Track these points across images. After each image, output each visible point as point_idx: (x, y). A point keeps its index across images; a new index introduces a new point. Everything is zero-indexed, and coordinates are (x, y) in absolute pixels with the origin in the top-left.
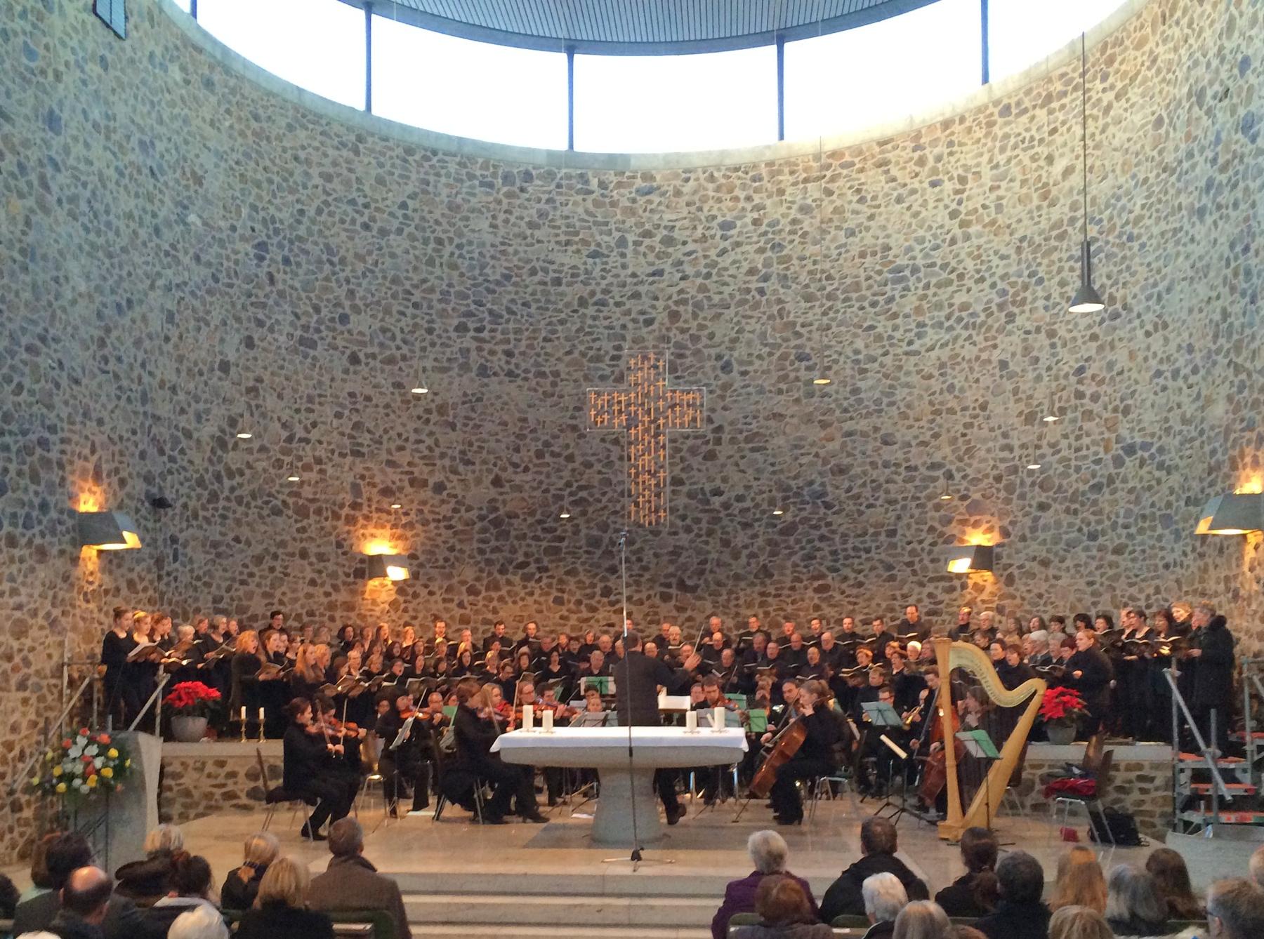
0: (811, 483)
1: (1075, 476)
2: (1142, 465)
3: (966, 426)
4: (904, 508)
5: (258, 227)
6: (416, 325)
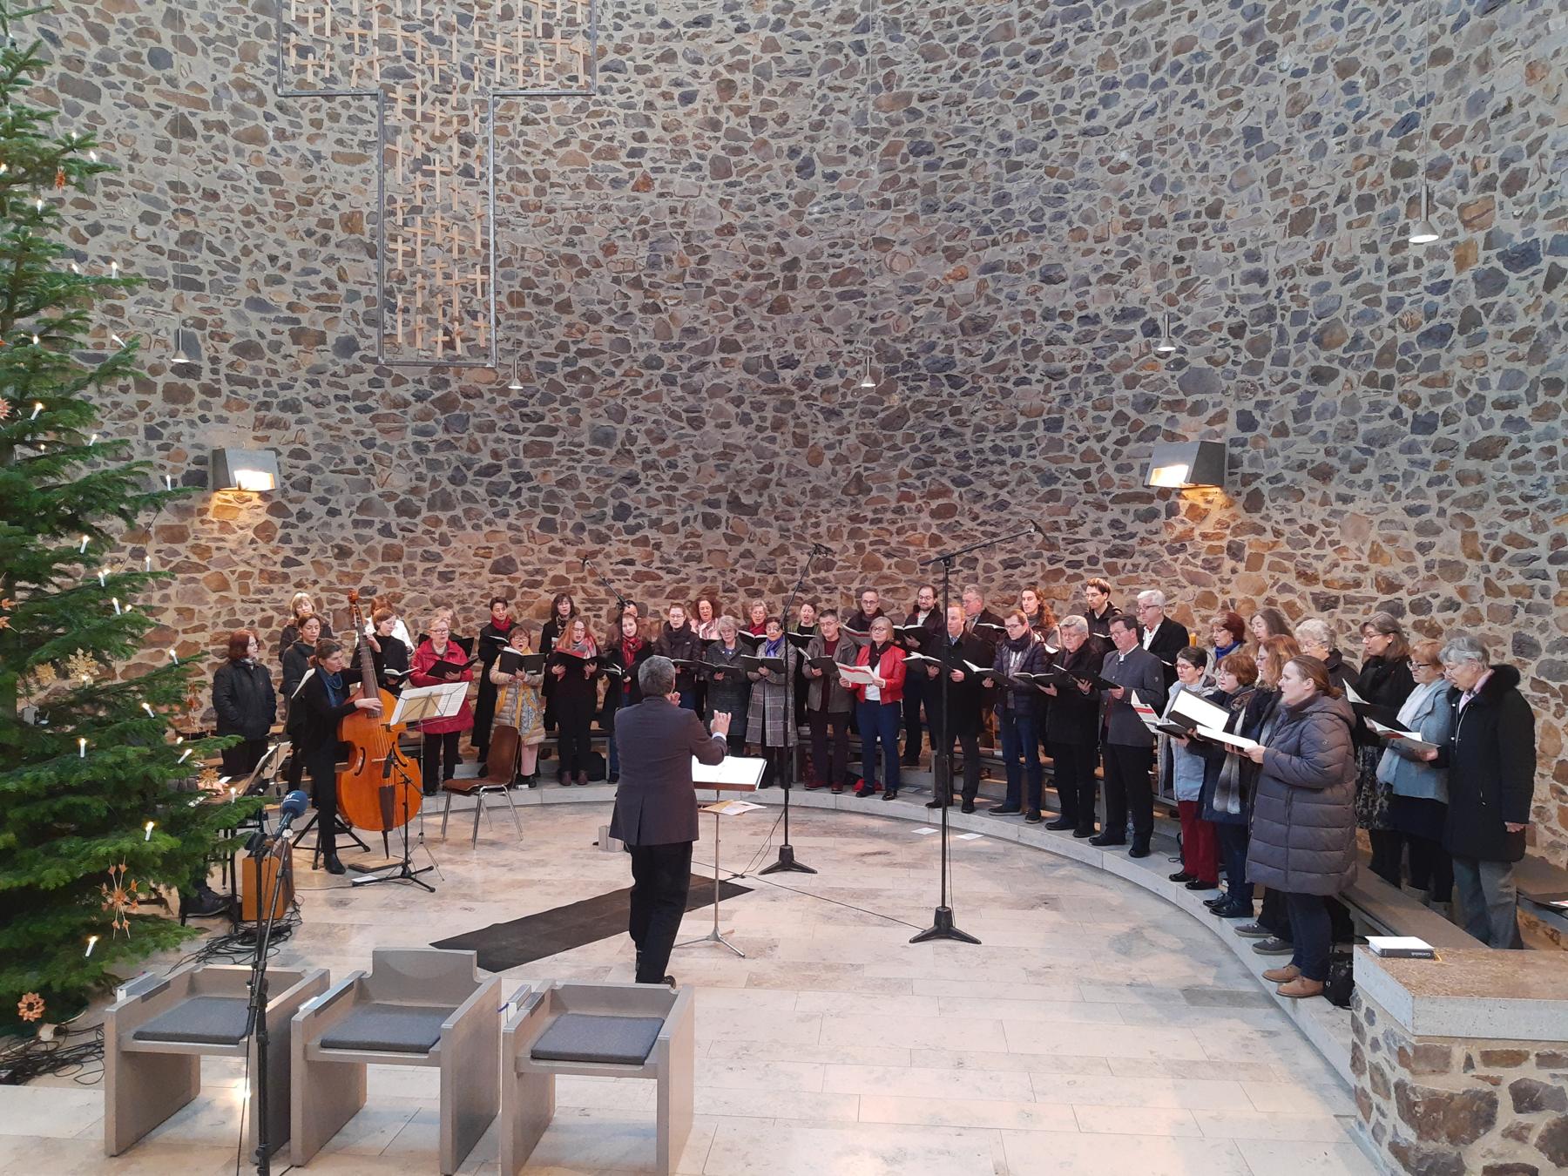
0: (932, 346)
1: (1388, 318)
3: (1182, 245)
4: (1076, 383)
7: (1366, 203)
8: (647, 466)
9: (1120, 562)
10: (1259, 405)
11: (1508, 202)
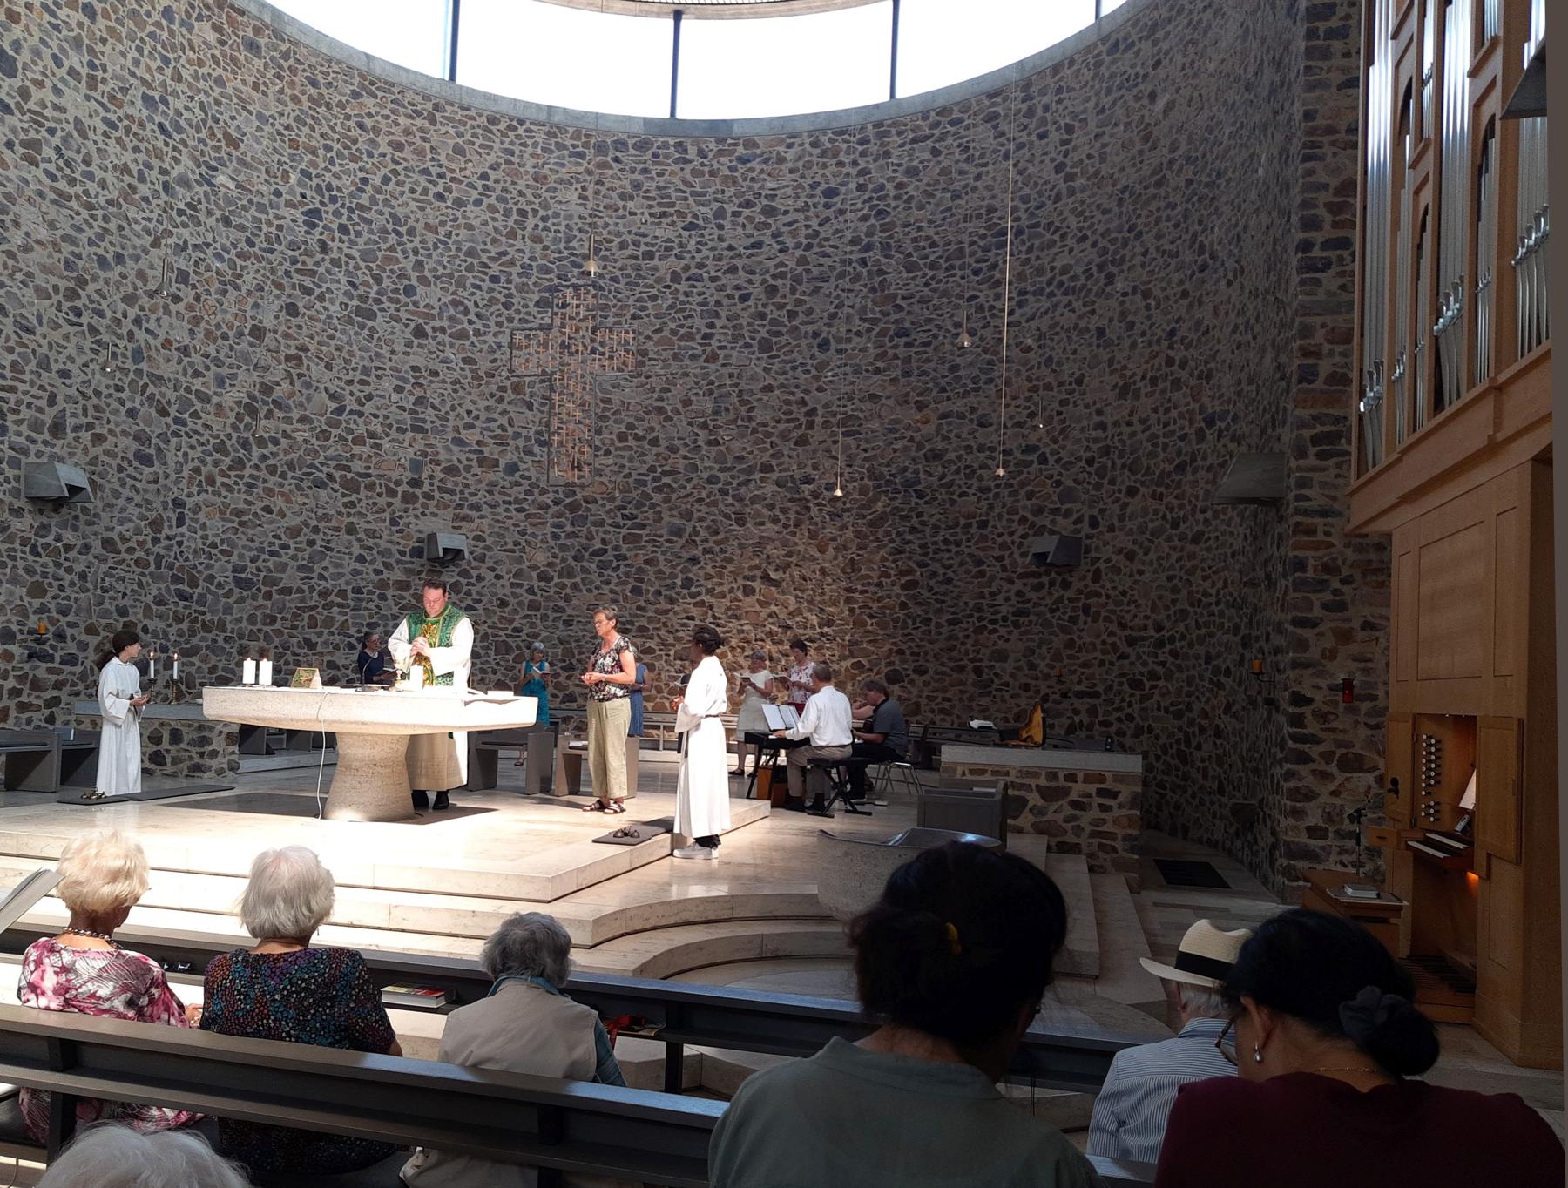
0: (905, 469)
5: (309, 194)
6: (493, 301)
8: (706, 551)
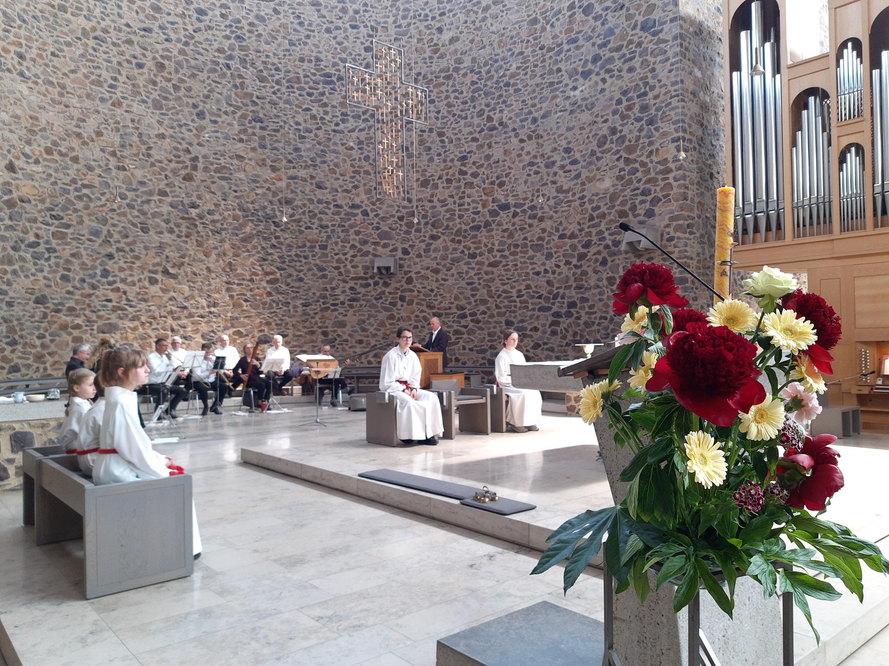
0: (265, 207)
2: (515, 215)
4: (333, 231)
7: (449, 181)
8: (119, 250)
9: (354, 303)
10: (410, 246)
11: (499, 190)
